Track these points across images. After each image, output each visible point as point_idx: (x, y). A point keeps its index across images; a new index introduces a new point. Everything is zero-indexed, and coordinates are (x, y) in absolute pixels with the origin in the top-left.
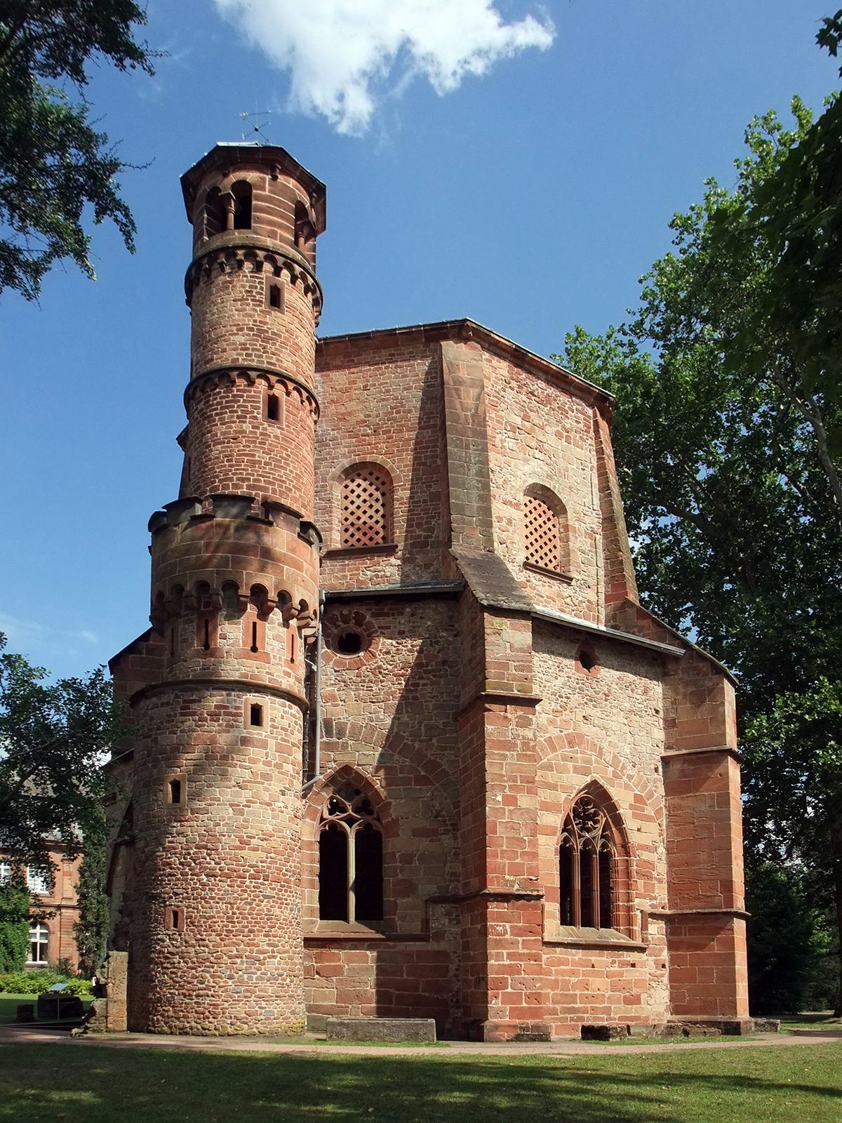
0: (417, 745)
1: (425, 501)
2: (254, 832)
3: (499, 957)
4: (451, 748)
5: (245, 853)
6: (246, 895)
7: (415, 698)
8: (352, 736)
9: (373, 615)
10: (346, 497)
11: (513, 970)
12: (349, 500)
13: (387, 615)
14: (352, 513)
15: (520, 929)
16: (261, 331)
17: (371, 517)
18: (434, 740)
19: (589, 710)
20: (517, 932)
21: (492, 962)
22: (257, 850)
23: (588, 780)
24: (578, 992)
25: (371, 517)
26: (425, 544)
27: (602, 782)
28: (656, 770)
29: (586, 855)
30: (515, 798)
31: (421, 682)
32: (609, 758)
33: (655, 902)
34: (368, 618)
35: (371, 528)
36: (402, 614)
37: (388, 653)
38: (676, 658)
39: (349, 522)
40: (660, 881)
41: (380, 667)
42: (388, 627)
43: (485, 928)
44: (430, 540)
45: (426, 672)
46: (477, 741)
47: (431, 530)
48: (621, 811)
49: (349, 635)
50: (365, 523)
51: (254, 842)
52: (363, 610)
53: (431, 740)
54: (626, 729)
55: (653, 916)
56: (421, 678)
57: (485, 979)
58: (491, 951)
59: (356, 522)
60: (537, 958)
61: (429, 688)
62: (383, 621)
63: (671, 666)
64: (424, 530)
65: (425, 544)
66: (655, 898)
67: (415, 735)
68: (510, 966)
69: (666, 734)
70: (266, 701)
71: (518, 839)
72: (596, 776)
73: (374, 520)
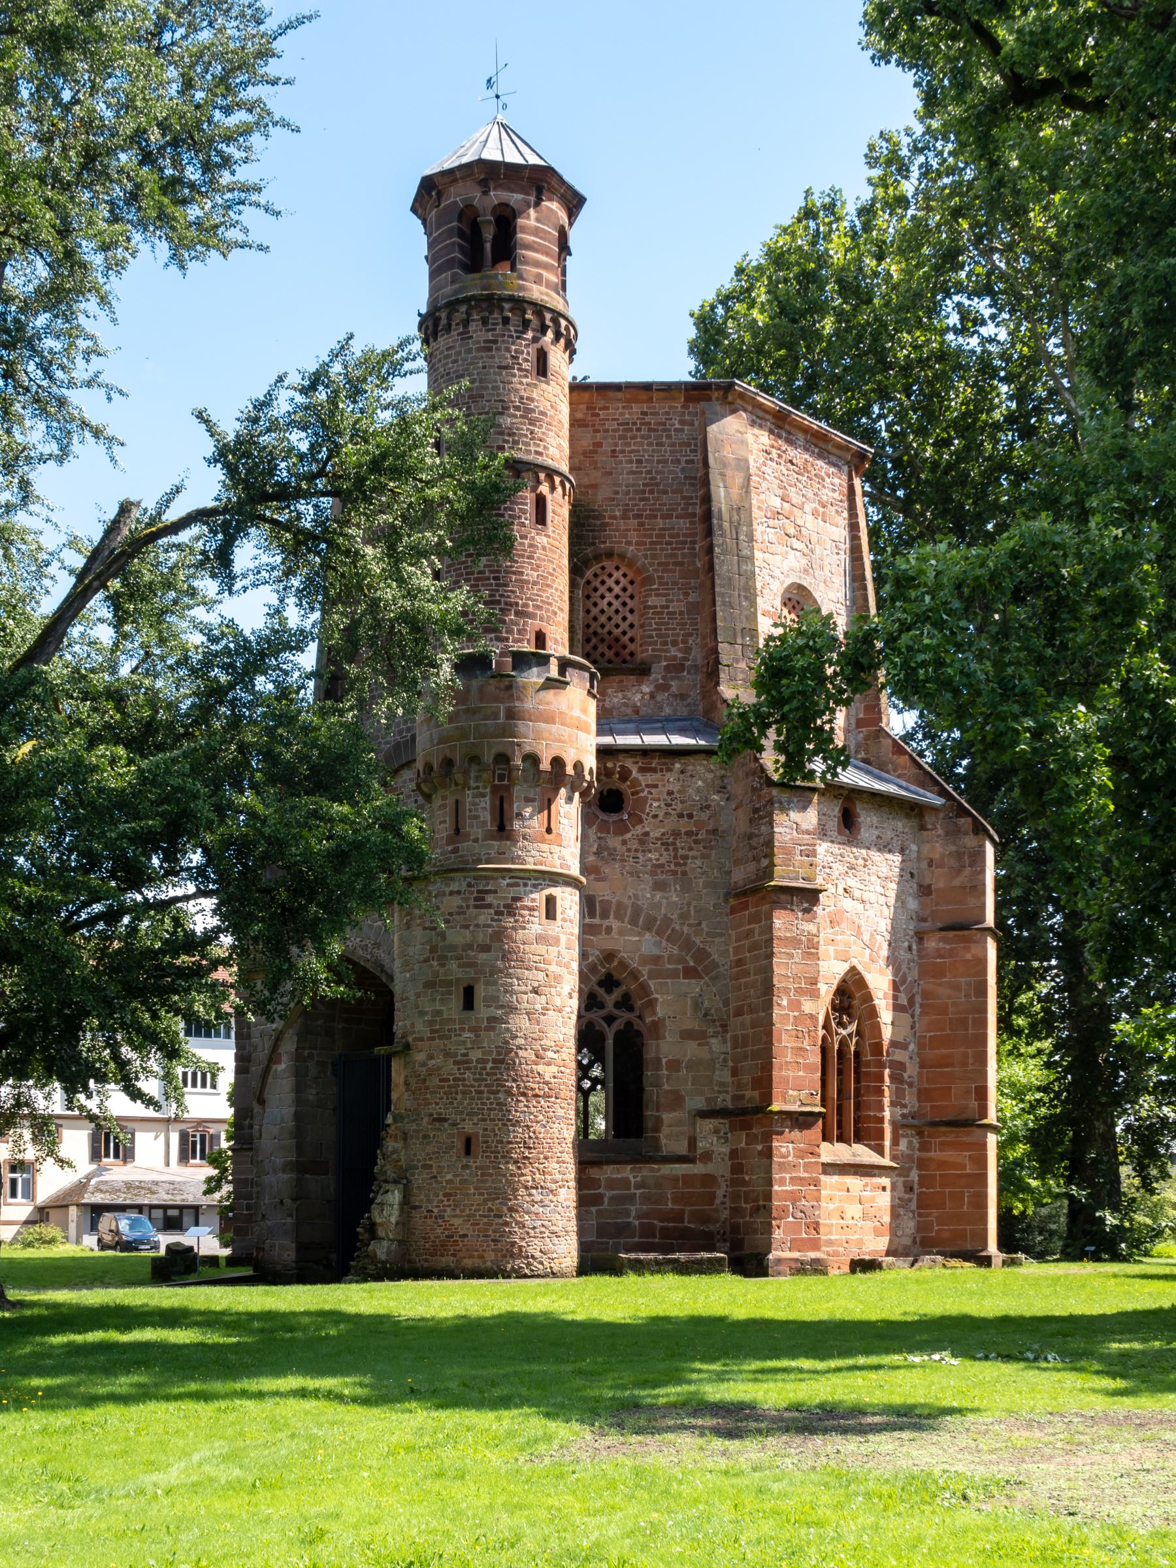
0: (686, 929)
1: (681, 613)
2: (549, 1043)
3: (782, 1182)
4: (721, 935)
5: (540, 1068)
6: (541, 1117)
7: (684, 873)
8: (619, 917)
9: (642, 770)
10: (588, 597)
11: (794, 1198)
12: (592, 600)
13: (654, 770)
14: (595, 619)
15: (801, 1151)
16: (529, 411)
17: (617, 626)
18: (704, 924)
19: (851, 882)
20: (801, 1154)
21: (776, 1188)
22: (549, 1064)
23: (846, 967)
24: (834, 1221)
25: (617, 626)
26: (680, 668)
27: (860, 968)
28: (910, 948)
29: (841, 1052)
30: (799, 1002)
31: (691, 854)
32: (866, 937)
33: (905, 1111)
34: (635, 773)
35: (617, 640)
36: (670, 770)
37: (655, 816)
38: (934, 809)
39: (591, 630)
40: (911, 1085)
41: (646, 834)
42: (656, 786)
43: (770, 1149)
44: (688, 663)
45: (696, 842)
46: (761, 934)
47: (687, 650)
48: (876, 1002)
49: (610, 791)
50: (610, 633)
51: (550, 1054)
52: (629, 763)
53: (700, 924)
54: (882, 900)
55: (904, 1126)
56: (691, 849)
57: (768, 1209)
58: (776, 1176)
59: (599, 630)
60: (817, 1183)
61: (698, 862)
62: (650, 778)
63: (929, 819)
64: (680, 650)
65: (680, 668)
66: (904, 1106)
67: (684, 916)
68: (792, 1192)
69: (921, 903)
70: (556, 891)
71: (801, 1049)
72: (855, 962)
73: (620, 630)
